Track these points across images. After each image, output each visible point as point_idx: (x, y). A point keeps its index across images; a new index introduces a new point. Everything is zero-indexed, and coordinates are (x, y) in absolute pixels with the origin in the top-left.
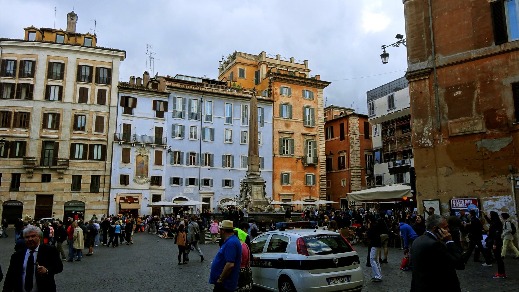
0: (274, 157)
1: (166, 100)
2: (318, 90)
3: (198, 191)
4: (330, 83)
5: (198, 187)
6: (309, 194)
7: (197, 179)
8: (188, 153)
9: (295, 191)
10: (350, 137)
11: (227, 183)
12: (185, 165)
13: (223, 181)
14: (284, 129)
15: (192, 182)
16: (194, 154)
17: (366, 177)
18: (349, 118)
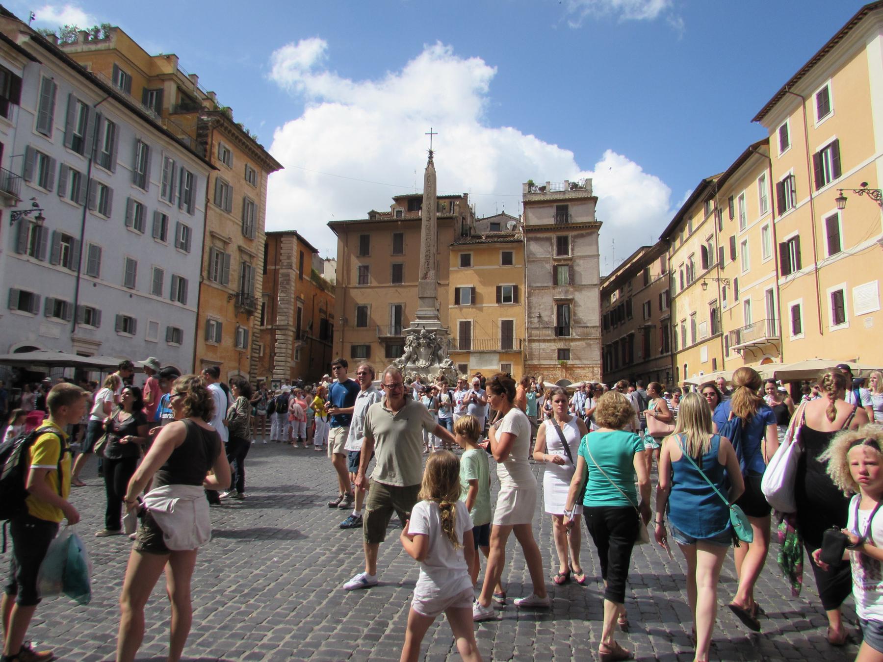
0: (200, 283)
1: (18, 73)
2: (264, 173)
3: (68, 334)
4: (282, 167)
5: (69, 326)
6: (237, 365)
7: (71, 305)
8: (54, 233)
9: (221, 358)
10: (281, 271)
11: (127, 324)
12: (46, 264)
13: (118, 317)
14: (217, 230)
15: (58, 308)
16: (67, 238)
17: (296, 345)
18: (282, 239)
